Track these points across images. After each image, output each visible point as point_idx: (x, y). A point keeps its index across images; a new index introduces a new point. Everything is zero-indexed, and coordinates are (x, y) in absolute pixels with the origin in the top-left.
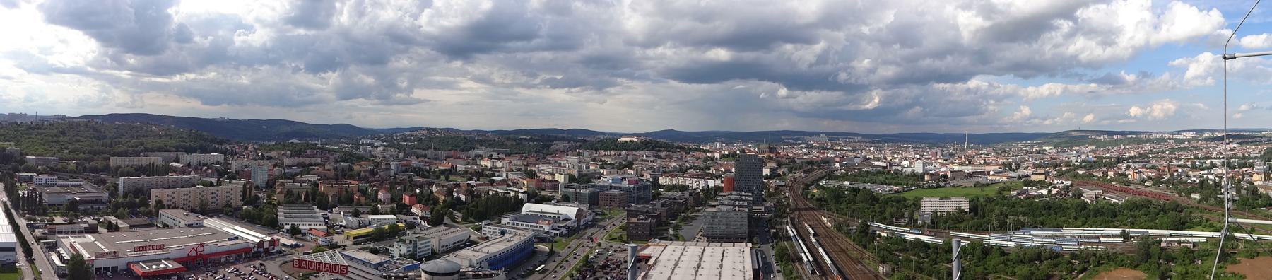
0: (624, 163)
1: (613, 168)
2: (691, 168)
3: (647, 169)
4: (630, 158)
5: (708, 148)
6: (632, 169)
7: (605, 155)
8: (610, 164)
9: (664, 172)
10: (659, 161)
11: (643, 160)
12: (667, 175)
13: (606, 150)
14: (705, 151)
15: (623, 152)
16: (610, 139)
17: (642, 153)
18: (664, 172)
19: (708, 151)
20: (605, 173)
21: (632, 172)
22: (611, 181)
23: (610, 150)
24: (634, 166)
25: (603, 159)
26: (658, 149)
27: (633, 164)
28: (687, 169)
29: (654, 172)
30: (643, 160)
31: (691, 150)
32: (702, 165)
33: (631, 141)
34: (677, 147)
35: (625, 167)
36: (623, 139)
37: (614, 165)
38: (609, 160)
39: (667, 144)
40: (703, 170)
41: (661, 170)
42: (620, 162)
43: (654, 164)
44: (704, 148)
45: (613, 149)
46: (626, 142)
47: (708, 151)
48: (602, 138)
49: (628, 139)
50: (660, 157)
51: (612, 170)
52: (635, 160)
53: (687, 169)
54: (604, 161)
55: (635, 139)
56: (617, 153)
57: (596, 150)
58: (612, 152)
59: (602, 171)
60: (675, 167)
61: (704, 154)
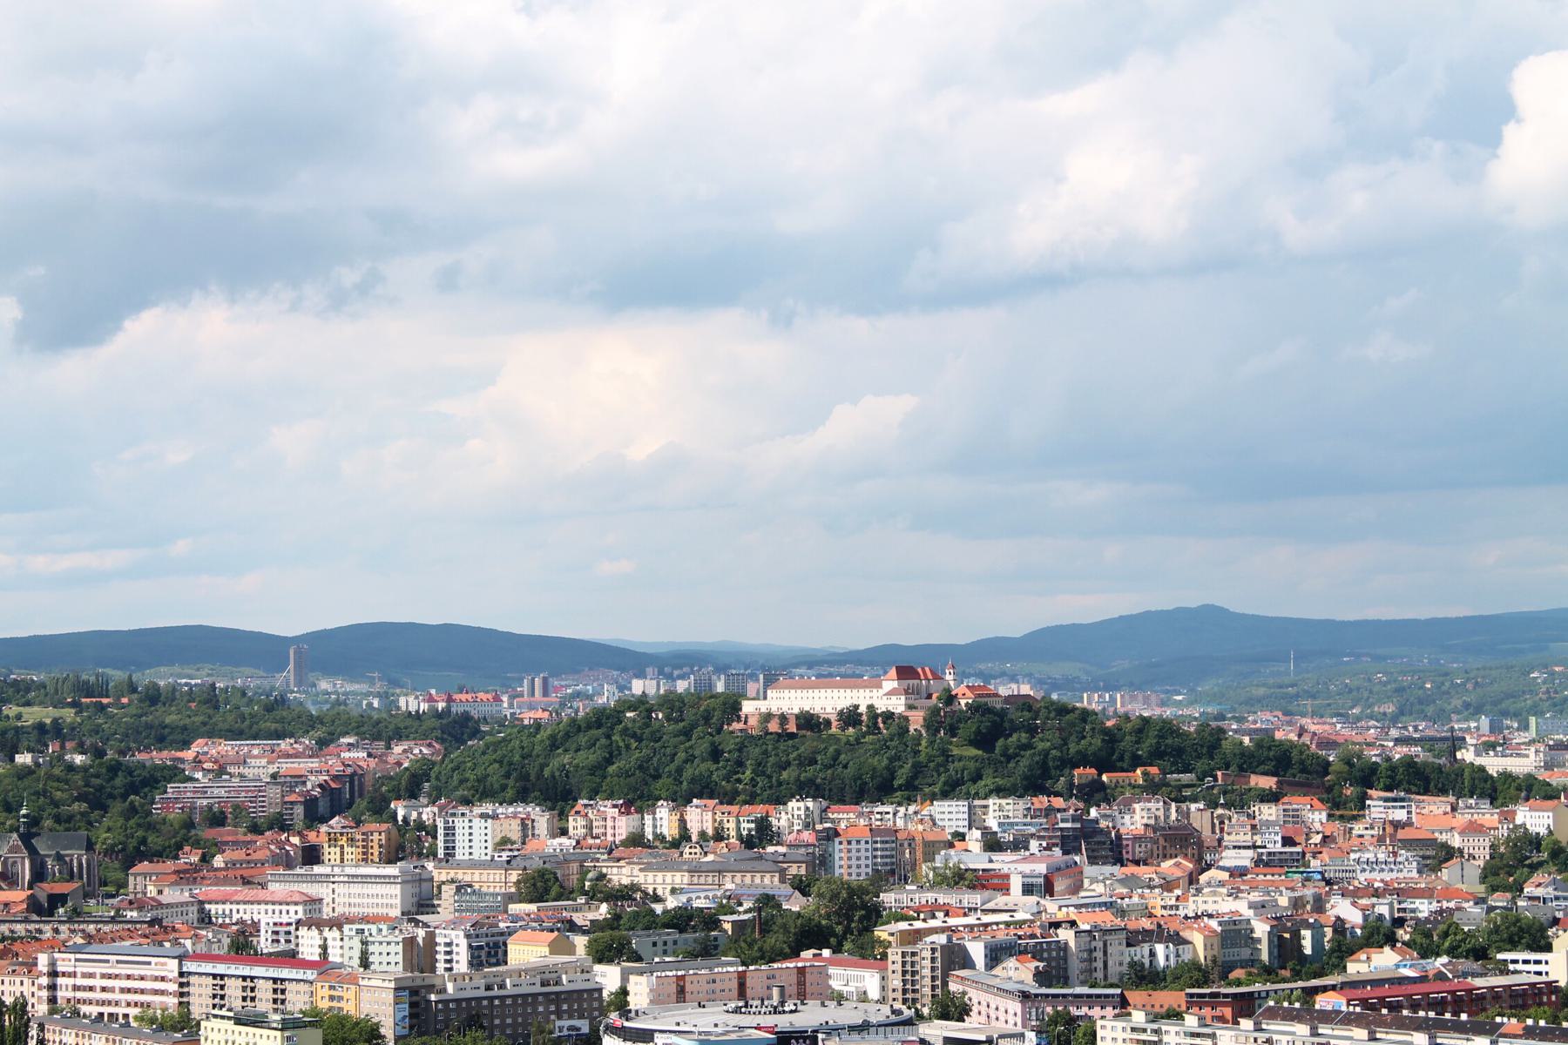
0: (795, 904)
1: (707, 951)
2: (1380, 934)
3: (995, 955)
4: (849, 864)
5: (1525, 763)
6: (869, 953)
7: (636, 840)
8: (682, 920)
9: (1147, 977)
10: (1099, 881)
11: (960, 878)
12: (1170, 998)
13: (638, 800)
14: (1500, 791)
15: (791, 816)
16: (672, 703)
17: (950, 814)
18: (1147, 977)
19: (1529, 789)
20: (640, 991)
21: (870, 981)
23: (681, 800)
24: (882, 933)
25: (621, 875)
26: (1082, 774)
27: (875, 915)
28: (1345, 945)
29: (1054, 969)
30: (960, 878)
31: (1367, 777)
32: (1472, 916)
33: (850, 717)
34: (1249, 762)
35: (811, 935)
36: (788, 701)
37: (710, 921)
39: (1167, 729)
40: (1480, 954)
41: (1120, 956)
42: (767, 901)
43: (1052, 907)
44: (1494, 764)
45: (704, 789)
46: (809, 722)
47: (1529, 789)
48: (607, 697)
49: (827, 701)
50: (1112, 850)
51: (698, 973)
52: (895, 873)
53: (1345, 945)
55: (885, 696)
56: (739, 821)
58: (699, 817)
59: (608, 977)
60: (1234, 934)
61: (1488, 815)
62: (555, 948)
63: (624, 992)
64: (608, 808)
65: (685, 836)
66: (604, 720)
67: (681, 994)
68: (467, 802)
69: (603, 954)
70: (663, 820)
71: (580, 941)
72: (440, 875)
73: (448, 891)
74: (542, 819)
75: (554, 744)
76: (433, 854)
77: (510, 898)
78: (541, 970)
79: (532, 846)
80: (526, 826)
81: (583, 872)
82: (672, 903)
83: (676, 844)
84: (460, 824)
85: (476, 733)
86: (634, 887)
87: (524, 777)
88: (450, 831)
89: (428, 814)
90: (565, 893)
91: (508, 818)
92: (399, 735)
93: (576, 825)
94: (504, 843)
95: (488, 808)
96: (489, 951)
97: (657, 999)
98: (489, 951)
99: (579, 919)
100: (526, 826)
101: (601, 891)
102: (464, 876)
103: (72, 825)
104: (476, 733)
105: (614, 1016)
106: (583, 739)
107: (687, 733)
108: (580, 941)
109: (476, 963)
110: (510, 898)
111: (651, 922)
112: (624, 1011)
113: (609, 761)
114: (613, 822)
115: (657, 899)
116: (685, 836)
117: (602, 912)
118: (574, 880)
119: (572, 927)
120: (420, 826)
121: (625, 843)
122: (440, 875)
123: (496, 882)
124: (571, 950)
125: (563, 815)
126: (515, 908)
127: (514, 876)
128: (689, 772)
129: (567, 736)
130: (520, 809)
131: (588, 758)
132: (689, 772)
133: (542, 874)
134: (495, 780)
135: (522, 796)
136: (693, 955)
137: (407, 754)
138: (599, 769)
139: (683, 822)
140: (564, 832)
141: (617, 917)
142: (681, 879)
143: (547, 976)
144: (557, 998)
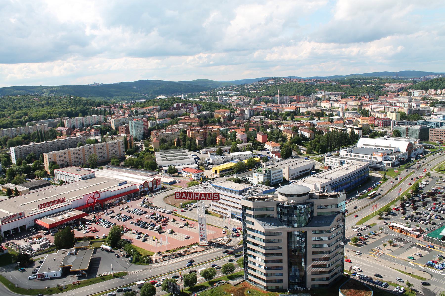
7: (436, 94)
8: (441, 102)
13: (436, 89)
20: (436, 110)
22: (442, 118)
23: (441, 89)
25: (434, 98)
38: (439, 99)
54: (434, 100)
57: (427, 89)
59: (432, 109)
62: (426, 105)
63: (434, 110)
64: (432, 90)
65: (441, 93)
66: (432, 81)
67: (441, 110)
68: (416, 90)
69: (431, 106)
70: (439, 91)
71: (429, 105)
72: (413, 97)
73: (413, 99)
74: (424, 91)
75: (426, 83)
76: (412, 95)
77: (421, 100)
78: (424, 108)
79: (423, 94)
80: (423, 92)
81: (429, 97)
82: (440, 101)
83: (440, 94)
84: (415, 92)
85: (417, 82)
86: (435, 99)
87: (422, 87)
88: (414, 93)
89: (411, 91)
90: (427, 100)
91: (421, 91)
92: (408, 83)
93: (428, 92)
94: (420, 94)
95: (418, 90)
96: (418, 106)
97: (438, 111)
98: (418, 106)
99: (428, 102)
100: (423, 92)
101: (431, 99)
102: (415, 98)
103: (352, 107)
104: (417, 82)
105: (433, 113)
106: (430, 83)
107: (442, 82)
108: (429, 105)
109: (416, 107)
110: (421, 100)
111: (437, 103)
112: (434, 112)
113: (433, 85)
114: (433, 92)
115: (438, 100)
116: (441, 93)
117: (431, 101)
118: (428, 98)
119: (428, 103)
120: (410, 92)
121: (434, 94)
122: (413, 97)
123: (419, 98)
124: (428, 106)
125: (427, 91)
126: (421, 101)
127: (421, 98)
128: (442, 86)
129: (428, 83)
130: (422, 90)
131: (430, 85)
132: (442, 86)
133: (424, 97)
134: (419, 87)
135: (422, 89)
136: (442, 106)
137: (409, 85)
138: (431, 86)
139: (441, 92)
140: (427, 93)
141: (433, 102)
142: (441, 98)
143: (425, 108)
144: (426, 111)
